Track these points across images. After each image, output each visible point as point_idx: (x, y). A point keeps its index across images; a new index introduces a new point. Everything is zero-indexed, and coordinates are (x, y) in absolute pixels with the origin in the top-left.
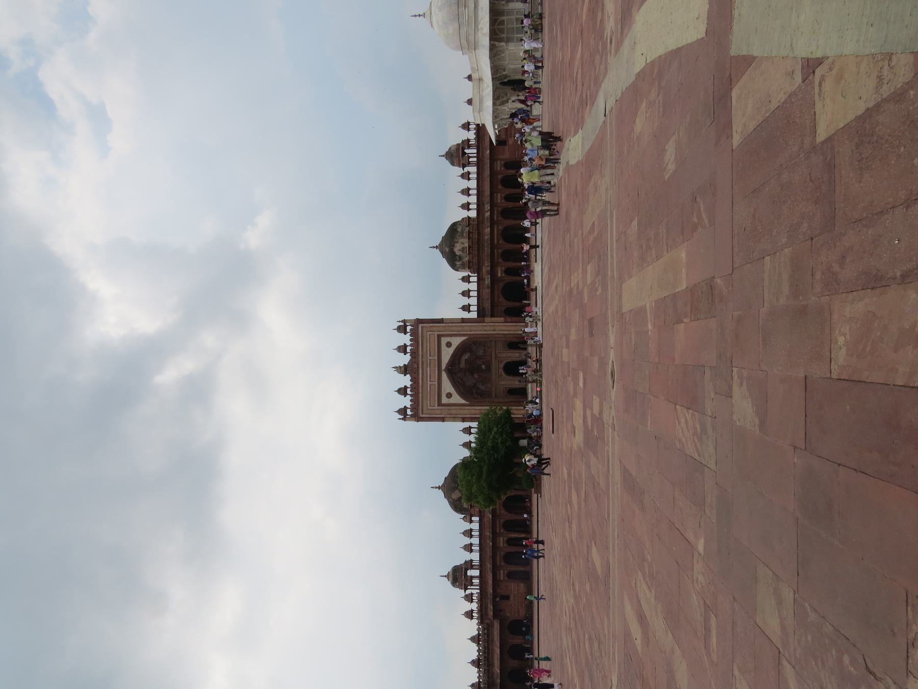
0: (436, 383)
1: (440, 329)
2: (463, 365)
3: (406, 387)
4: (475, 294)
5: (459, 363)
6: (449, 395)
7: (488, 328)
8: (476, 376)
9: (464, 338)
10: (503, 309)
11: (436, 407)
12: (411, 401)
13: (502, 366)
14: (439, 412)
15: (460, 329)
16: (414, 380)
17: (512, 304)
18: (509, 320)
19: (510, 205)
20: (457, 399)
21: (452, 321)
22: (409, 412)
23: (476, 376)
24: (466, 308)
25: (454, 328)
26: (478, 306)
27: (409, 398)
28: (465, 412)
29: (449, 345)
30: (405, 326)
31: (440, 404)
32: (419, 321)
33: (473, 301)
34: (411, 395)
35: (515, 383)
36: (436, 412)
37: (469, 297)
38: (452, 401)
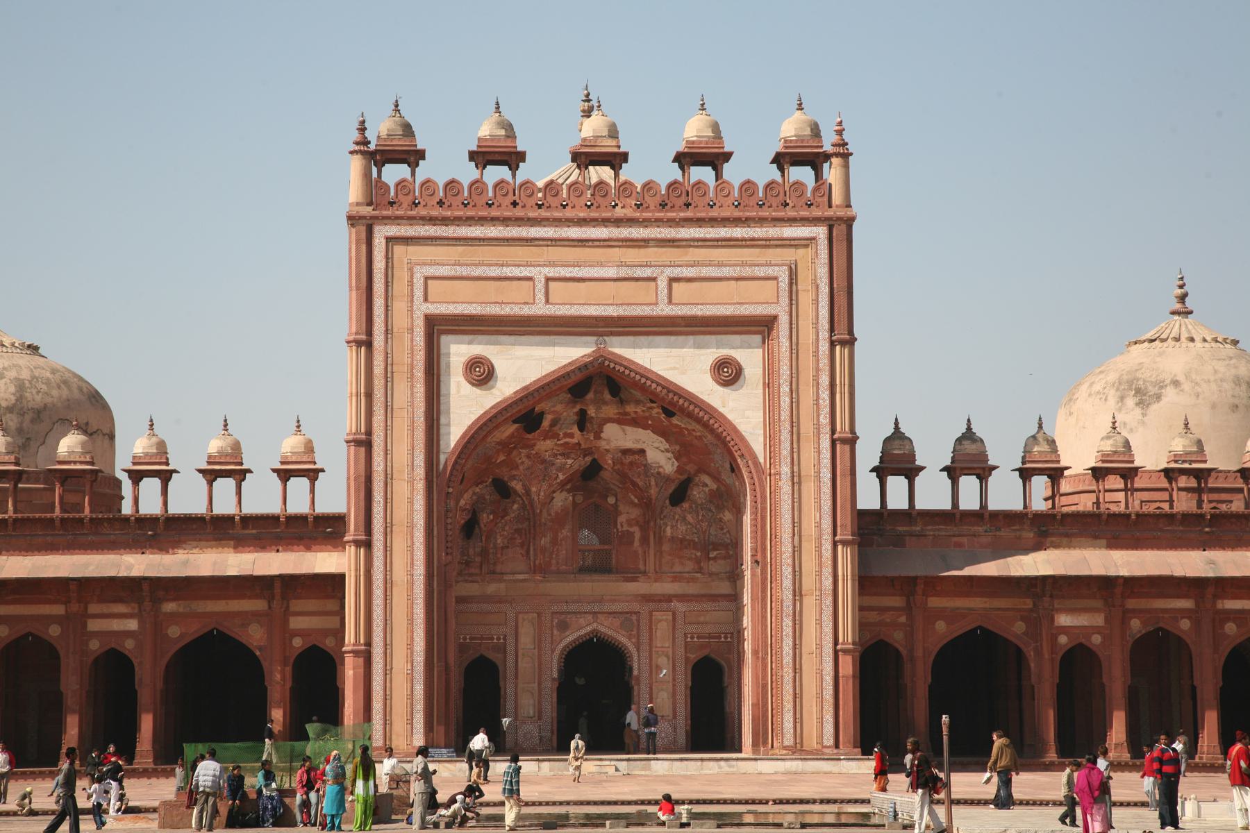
0: (540, 309)
2: (617, 437)
3: (513, 159)
4: (969, 500)
5: (624, 420)
8: (561, 500)
10: (897, 638)
11: (422, 309)
12: (452, 184)
14: (400, 320)
15: (807, 427)
16: (548, 204)
18: (847, 666)
21: (842, 389)
22: (393, 173)
23: (561, 500)
24: (898, 460)
26: (911, 515)
27: (467, 173)
30: (815, 161)
32: (841, 229)
33: (933, 493)
34: (477, 185)
35: (530, 692)
36: (399, 306)
37: (953, 472)
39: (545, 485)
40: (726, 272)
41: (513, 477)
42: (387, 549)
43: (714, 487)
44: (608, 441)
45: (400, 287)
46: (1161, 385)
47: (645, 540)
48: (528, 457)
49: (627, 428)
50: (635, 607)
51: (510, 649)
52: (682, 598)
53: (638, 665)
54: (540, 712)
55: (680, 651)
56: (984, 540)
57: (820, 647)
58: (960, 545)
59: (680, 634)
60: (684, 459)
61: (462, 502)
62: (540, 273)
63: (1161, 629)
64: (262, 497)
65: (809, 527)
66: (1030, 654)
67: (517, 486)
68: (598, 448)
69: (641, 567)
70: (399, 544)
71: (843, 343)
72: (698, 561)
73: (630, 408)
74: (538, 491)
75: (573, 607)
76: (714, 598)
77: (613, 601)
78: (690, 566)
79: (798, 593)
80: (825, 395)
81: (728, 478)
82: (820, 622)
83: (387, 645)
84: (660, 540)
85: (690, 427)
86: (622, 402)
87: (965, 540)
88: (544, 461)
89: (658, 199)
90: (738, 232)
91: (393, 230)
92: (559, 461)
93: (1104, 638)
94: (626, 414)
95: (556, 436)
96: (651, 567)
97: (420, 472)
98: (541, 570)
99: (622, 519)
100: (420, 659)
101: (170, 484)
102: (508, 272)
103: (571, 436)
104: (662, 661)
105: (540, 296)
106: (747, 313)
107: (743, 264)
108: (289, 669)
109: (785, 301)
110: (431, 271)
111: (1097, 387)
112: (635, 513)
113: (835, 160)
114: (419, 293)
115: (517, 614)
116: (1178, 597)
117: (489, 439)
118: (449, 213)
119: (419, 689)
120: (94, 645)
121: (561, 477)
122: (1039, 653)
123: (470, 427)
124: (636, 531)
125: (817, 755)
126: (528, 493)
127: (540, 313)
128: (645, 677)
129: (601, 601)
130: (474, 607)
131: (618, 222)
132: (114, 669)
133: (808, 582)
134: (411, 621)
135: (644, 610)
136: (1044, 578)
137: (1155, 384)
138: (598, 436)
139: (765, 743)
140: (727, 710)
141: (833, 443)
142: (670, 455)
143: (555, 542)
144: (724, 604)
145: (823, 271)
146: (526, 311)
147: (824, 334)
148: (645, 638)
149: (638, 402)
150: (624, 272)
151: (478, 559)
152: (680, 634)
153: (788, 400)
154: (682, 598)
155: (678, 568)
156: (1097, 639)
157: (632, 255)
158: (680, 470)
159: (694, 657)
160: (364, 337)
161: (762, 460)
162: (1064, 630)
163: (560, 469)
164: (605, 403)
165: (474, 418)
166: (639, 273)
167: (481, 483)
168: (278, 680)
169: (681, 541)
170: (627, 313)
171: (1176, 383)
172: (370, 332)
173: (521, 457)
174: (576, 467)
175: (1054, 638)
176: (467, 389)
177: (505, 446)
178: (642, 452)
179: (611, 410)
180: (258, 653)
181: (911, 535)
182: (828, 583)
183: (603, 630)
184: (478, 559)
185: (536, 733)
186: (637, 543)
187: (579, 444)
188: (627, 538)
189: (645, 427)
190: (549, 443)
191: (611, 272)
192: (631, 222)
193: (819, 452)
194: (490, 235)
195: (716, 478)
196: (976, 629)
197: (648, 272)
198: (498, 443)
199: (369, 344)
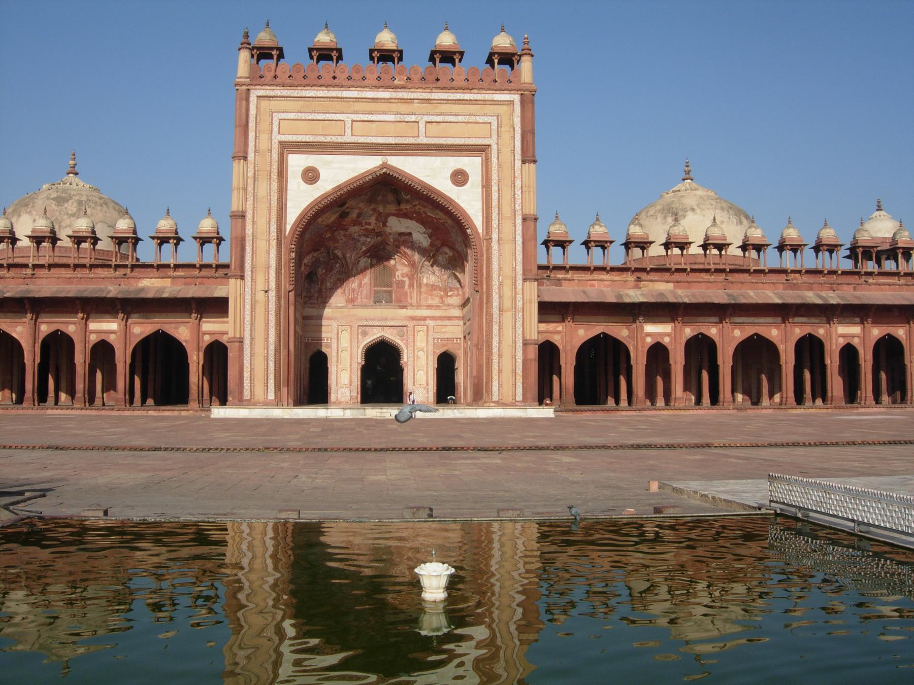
0: (348, 138)
1: (506, 152)
6: (311, 175)
7: (507, 292)
9: (478, 221)
10: (556, 339)
11: (277, 138)
13: (391, 336)
14: (264, 145)
17: (568, 363)
19: (832, 361)
20: (301, 199)
25: (507, 193)
28: (262, 222)
29: (459, 178)
31: (287, 148)
36: (264, 137)
38: (295, 183)
39: (354, 254)
40: (461, 119)
41: (336, 248)
42: (253, 280)
43: (451, 254)
44: (391, 228)
45: (264, 126)
46: (685, 210)
47: (411, 285)
48: (345, 236)
49: (402, 219)
50: (405, 323)
51: (334, 346)
52: (433, 318)
53: (406, 358)
54: (351, 382)
55: (431, 348)
56: (606, 283)
57: (515, 342)
58: (593, 286)
59: (431, 339)
60: (434, 238)
61: (305, 261)
62: (348, 118)
63: (701, 334)
64: (189, 253)
65: (507, 271)
66: (631, 349)
67: (339, 254)
68: (385, 232)
69: (409, 300)
70: (260, 279)
71: (530, 162)
72: (442, 298)
73: (403, 206)
74: (351, 256)
75: (370, 323)
76: (450, 318)
77: (393, 319)
78: (436, 301)
79: (501, 310)
80: (518, 192)
81: (459, 247)
82: (515, 327)
83: (252, 339)
84: (420, 285)
85: (438, 217)
86: (399, 203)
87: (595, 282)
88: (354, 239)
89: (419, 76)
90: (467, 96)
91: (262, 93)
92: (363, 239)
93: (671, 339)
94: (400, 210)
95: (360, 224)
96: (414, 301)
97: (274, 235)
98: (351, 301)
99: (398, 273)
100: (272, 348)
101: (138, 246)
102: (329, 116)
103: (369, 224)
104: (421, 354)
105: (348, 131)
106: (472, 143)
107: (470, 115)
108: (201, 355)
109: (495, 137)
110: (284, 116)
111: (651, 213)
112: (406, 270)
113: (524, 58)
114: (275, 129)
115: (338, 326)
116: (710, 316)
117: (319, 220)
118: (296, 83)
119: (272, 365)
120: (94, 338)
121: (364, 248)
122: (636, 348)
123: (305, 209)
124: (406, 280)
125: (513, 405)
126: (345, 257)
127: (348, 141)
128: (411, 361)
129: (386, 319)
130: (313, 322)
131: (396, 87)
132: (103, 352)
133: (507, 304)
134: (267, 324)
135: (411, 324)
136: (642, 304)
137: (682, 210)
138: (385, 225)
139: (481, 398)
140: (456, 381)
141: (524, 219)
142: (426, 235)
143: (360, 285)
144: (456, 322)
145: (517, 121)
146: (340, 139)
147: (518, 157)
148: (411, 340)
149: (407, 201)
150: (399, 118)
151: (316, 295)
152: (431, 339)
153: (496, 195)
154: (433, 318)
155: (430, 302)
156: (666, 340)
157: (403, 108)
158: (431, 245)
159: (439, 351)
160: (242, 154)
161: (480, 231)
162: (649, 335)
163: (363, 244)
164: (388, 203)
165: (307, 203)
166: (408, 118)
167: (318, 250)
168: (196, 360)
169: (432, 286)
170: (400, 142)
171: (693, 210)
172: (246, 152)
173: (340, 236)
174: (372, 243)
175: (643, 339)
176: (304, 186)
177: (332, 228)
178: (410, 234)
179: (392, 208)
180: (184, 344)
181: (566, 280)
182: (520, 304)
183: (387, 335)
184: (316, 295)
185: (348, 393)
186: (407, 287)
187: (374, 229)
188: (401, 284)
189: (412, 219)
190: (356, 228)
191: (392, 118)
192: (403, 87)
193: (515, 226)
194: (319, 95)
195: (452, 248)
196: (600, 335)
197: (413, 118)
198: (326, 226)
199: (245, 158)
